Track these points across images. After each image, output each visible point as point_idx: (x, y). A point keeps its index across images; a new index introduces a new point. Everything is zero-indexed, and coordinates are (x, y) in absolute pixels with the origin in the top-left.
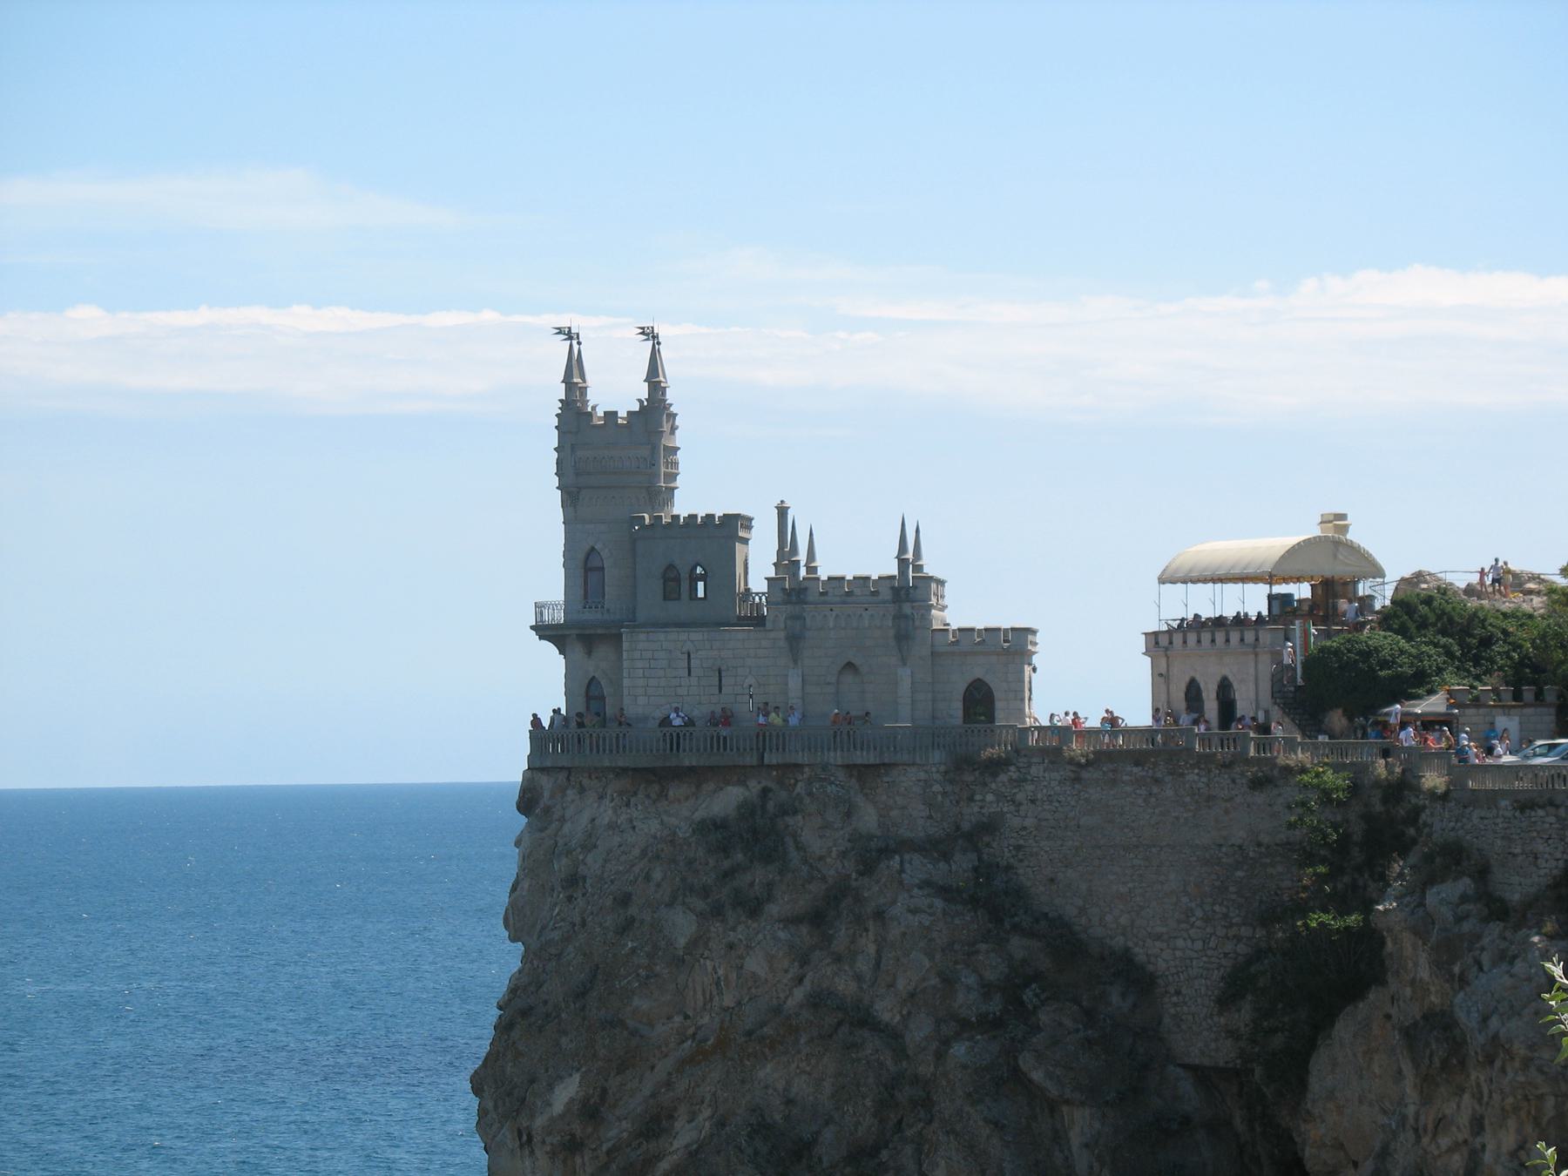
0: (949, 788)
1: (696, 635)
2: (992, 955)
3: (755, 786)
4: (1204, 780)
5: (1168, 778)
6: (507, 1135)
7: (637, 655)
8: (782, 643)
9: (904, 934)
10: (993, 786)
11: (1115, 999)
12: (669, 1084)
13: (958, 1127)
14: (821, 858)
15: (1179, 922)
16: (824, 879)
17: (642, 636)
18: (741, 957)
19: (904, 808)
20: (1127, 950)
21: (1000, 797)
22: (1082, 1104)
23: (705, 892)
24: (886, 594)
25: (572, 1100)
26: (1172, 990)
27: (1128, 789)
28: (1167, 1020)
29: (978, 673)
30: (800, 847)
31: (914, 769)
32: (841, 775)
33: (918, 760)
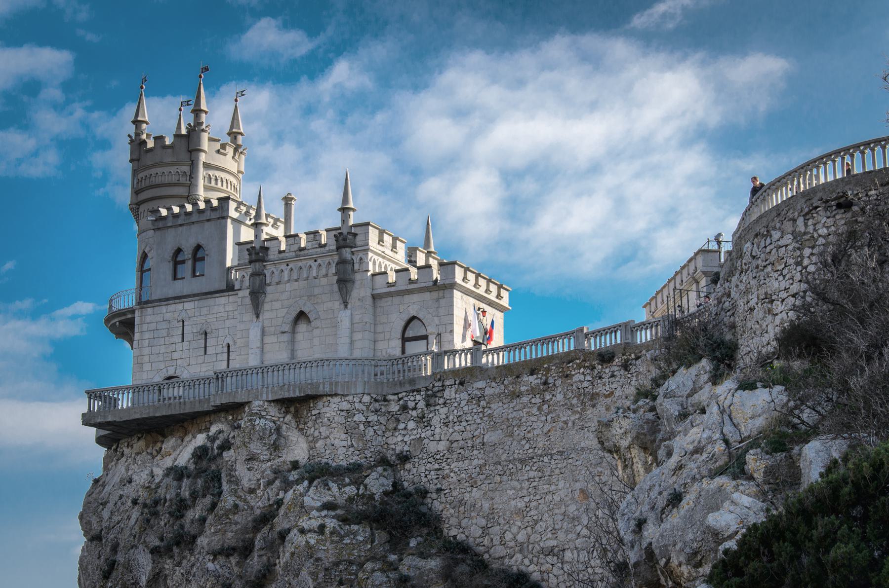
0: (373, 418)
1: (189, 305)
2: (379, 574)
4: (589, 378)
7: (145, 327)
8: (248, 301)
9: (293, 554)
10: (414, 413)
14: (252, 491)
16: (252, 508)
17: (149, 310)
19: (326, 438)
27: (525, 399)
29: (413, 313)
30: (235, 481)
31: (336, 399)
32: (273, 411)
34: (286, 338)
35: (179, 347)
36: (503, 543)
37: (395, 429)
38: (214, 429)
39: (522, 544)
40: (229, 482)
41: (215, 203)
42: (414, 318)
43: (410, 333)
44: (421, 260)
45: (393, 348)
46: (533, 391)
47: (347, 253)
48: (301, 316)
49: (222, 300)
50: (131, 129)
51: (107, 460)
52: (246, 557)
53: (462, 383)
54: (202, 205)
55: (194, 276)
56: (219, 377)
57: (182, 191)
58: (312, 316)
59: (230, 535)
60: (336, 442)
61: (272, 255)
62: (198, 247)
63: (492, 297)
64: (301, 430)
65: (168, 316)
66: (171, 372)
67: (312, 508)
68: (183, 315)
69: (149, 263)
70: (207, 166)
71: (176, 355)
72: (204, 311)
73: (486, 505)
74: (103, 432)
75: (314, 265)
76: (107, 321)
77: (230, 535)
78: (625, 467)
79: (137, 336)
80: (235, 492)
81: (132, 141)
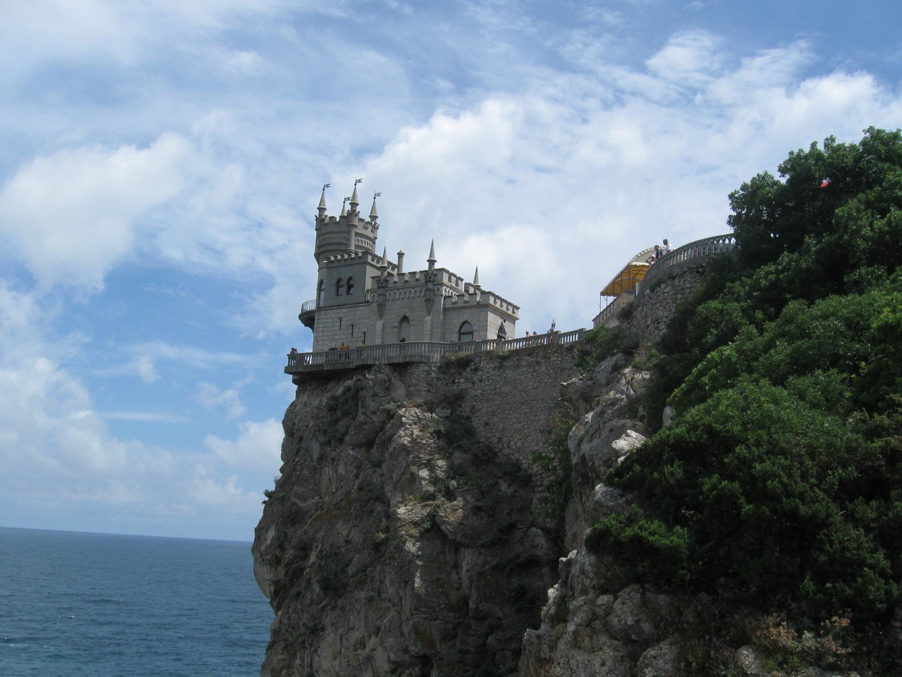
0: (441, 376)
1: (344, 310)
3: (355, 379)
5: (543, 361)
6: (259, 555)
8: (376, 309)
11: (504, 487)
12: (305, 532)
13: (396, 555)
14: (374, 413)
15: (544, 443)
18: (337, 465)
19: (416, 385)
20: (517, 460)
21: (466, 379)
22: (468, 546)
23: (325, 432)
24: (423, 280)
25: (273, 538)
26: (539, 483)
27: (524, 369)
28: (535, 501)
31: (422, 365)
32: (387, 370)
33: (424, 360)
34: (396, 330)
35: (338, 333)
36: (509, 447)
37: (453, 382)
38: (355, 379)
39: (519, 448)
40: (363, 407)
41: (360, 254)
42: (466, 322)
43: (463, 330)
44: (471, 291)
45: (455, 338)
46: (530, 365)
47: (430, 286)
48: (405, 319)
49: (363, 308)
50: (317, 213)
51: (298, 392)
52: (370, 448)
53: (491, 359)
54: (353, 256)
55: (348, 292)
56: (359, 350)
57: (342, 248)
58: (410, 319)
59: (362, 436)
60: (421, 388)
61: (391, 285)
62: (350, 279)
63: (510, 312)
64: (402, 381)
65: (332, 316)
66: (333, 345)
67: (406, 424)
68: (341, 315)
69: (323, 287)
70: (357, 234)
71: (336, 337)
72: (352, 314)
73: (501, 426)
74: (296, 377)
75: (413, 291)
76: (301, 317)
77: (362, 436)
78: (575, 410)
79: (315, 326)
80: (365, 413)
81: (317, 219)
